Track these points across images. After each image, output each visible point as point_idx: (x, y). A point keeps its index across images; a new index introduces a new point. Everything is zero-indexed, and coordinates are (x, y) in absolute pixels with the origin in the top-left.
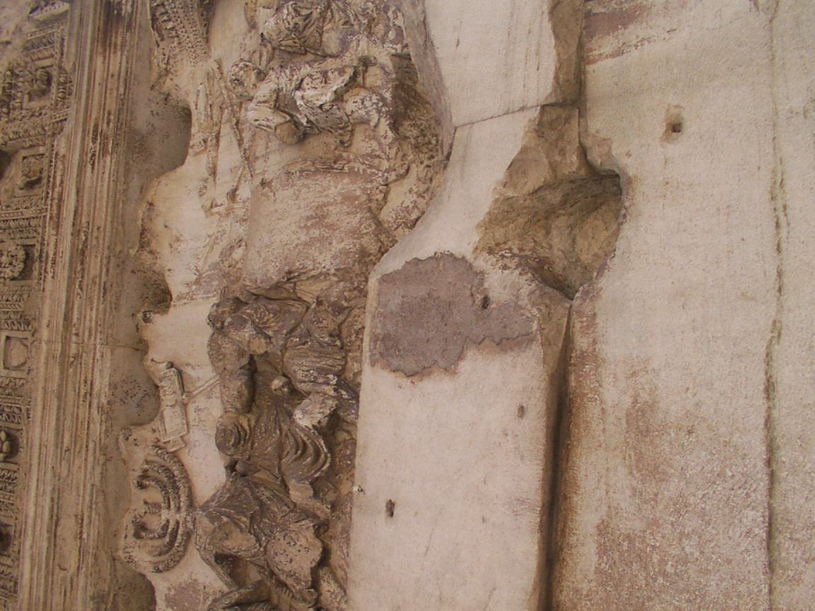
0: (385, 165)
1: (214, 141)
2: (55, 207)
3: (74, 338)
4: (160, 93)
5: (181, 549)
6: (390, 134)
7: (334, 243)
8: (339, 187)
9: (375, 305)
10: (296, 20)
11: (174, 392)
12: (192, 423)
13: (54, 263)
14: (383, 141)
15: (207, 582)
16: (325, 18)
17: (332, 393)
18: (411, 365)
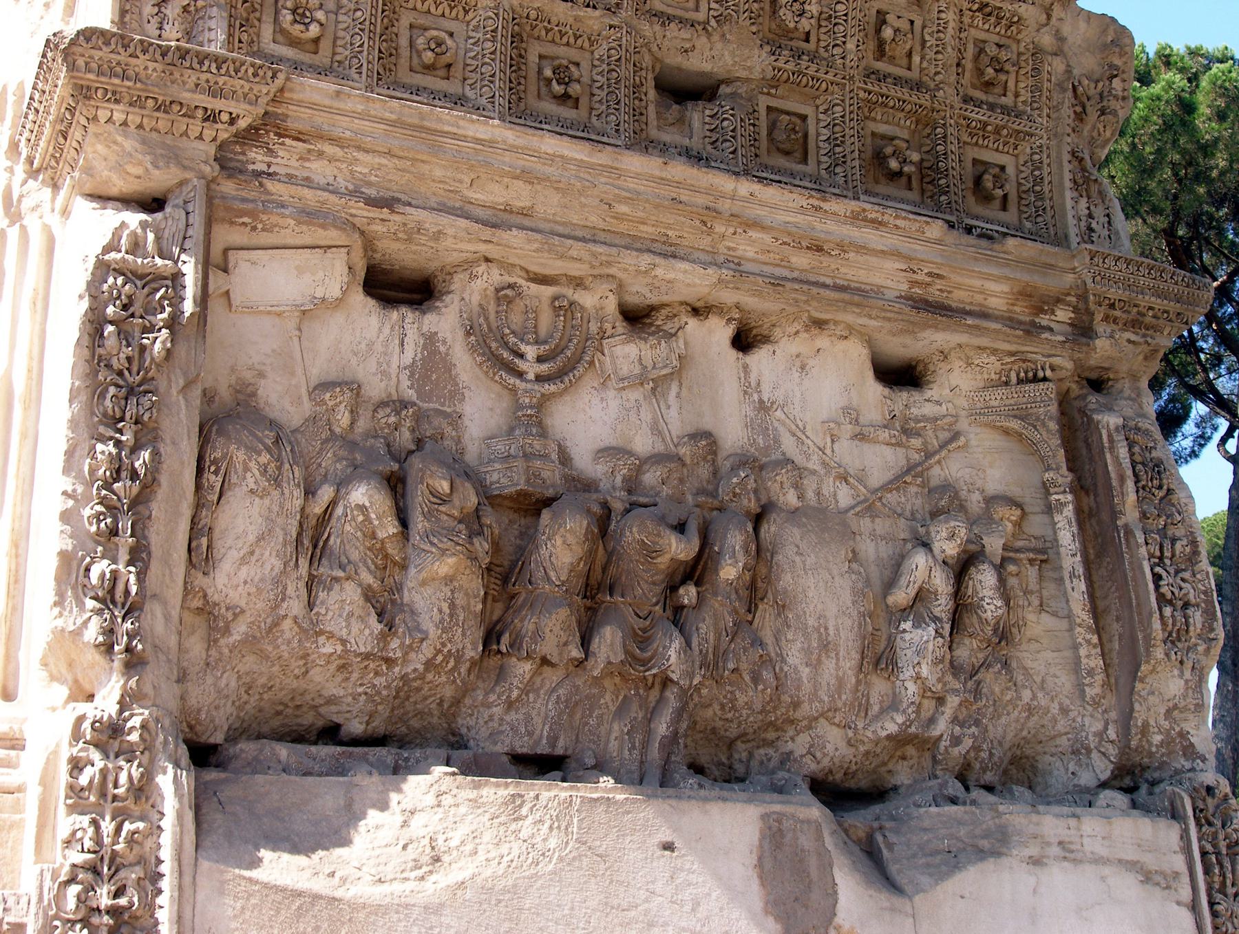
0: (860, 725)
1: (893, 441)
2: (873, 216)
3: (731, 230)
4: (951, 349)
5: (497, 378)
6: (884, 734)
7: (807, 670)
8: (850, 672)
9: (801, 816)
10: (989, 613)
11: (654, 367)
12: (624, 393)
13: (817, 209)
14: (879, 724)
15: (467, 422)
16: (981, 641)
17: (695, 682)
18: (768, 864)
